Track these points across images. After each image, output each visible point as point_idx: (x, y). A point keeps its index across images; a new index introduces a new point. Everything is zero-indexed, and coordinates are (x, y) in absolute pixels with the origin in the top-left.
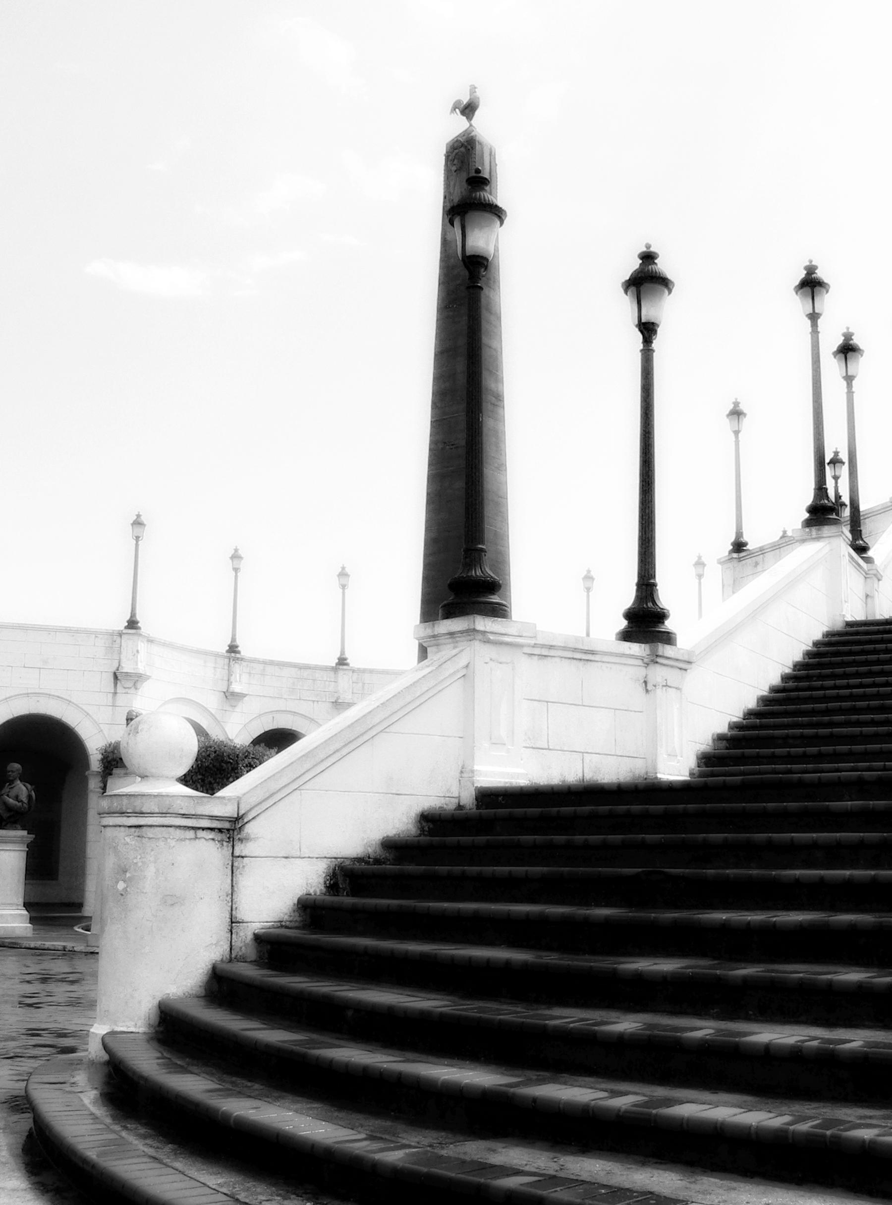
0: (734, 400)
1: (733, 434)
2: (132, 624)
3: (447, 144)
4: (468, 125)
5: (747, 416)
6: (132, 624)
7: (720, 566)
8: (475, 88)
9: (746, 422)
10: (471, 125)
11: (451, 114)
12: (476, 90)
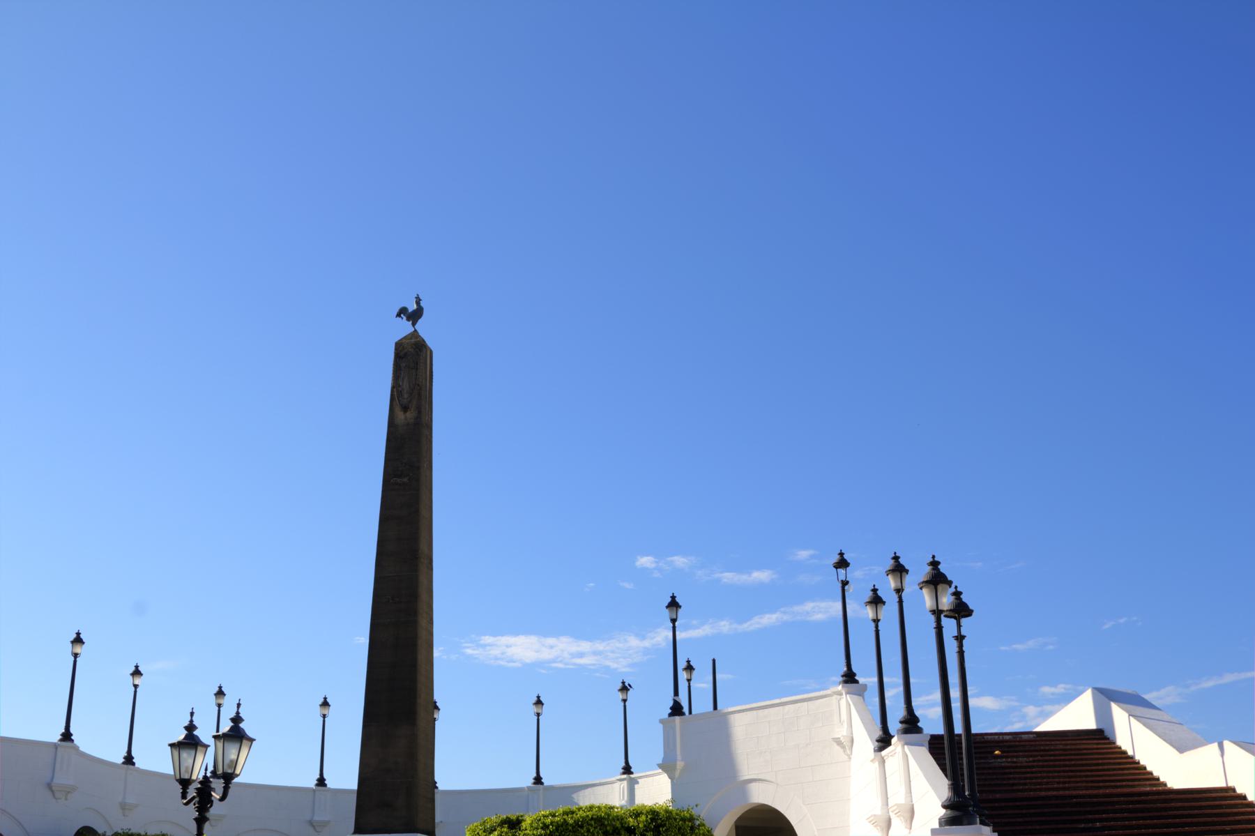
2: (67, 736)
3: (396, 344)
4: (413, 330)
6: (67, 736)
7: (661, 725)
9: (680, 611)
10: (415, 330)
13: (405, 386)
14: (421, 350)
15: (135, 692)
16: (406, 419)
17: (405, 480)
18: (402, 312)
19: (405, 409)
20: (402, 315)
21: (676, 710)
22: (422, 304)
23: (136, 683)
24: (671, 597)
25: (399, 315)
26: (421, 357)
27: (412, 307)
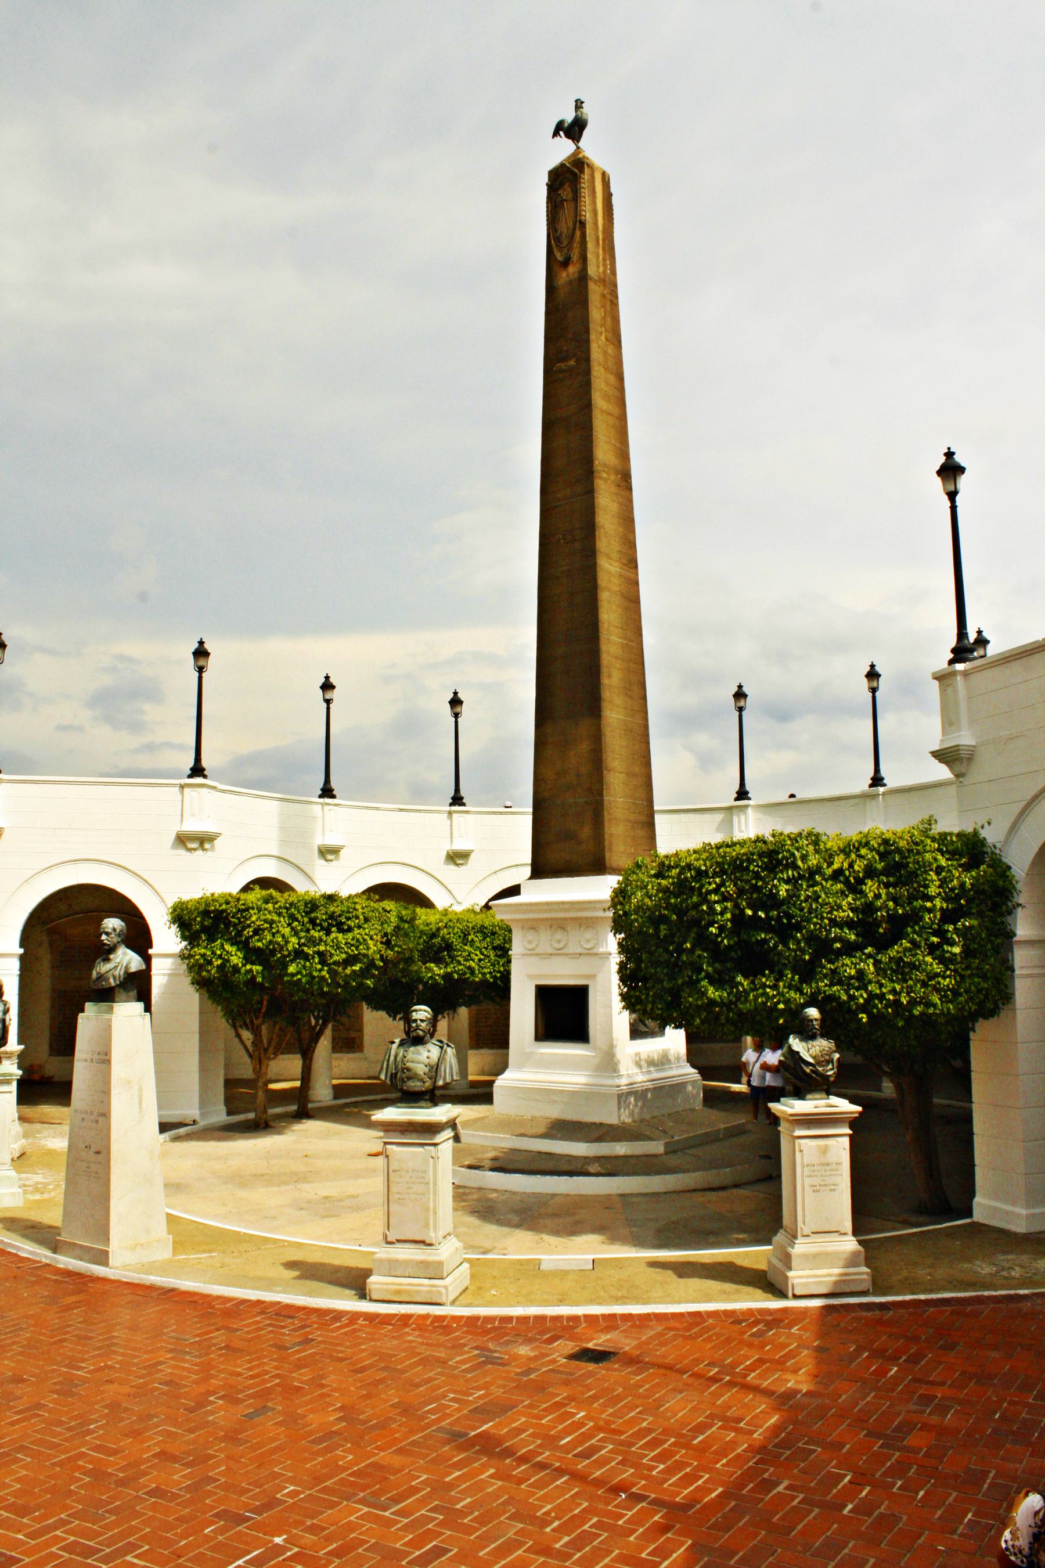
0: (947, 451)
1: (946, 497)
3: (550, 173)
4: (574, 147)
5: (966, 472)
7: (936, 683)
8: (582, 102)
10: (578, 148)
11: (553, 137)
12: (583, 105)
13: (565, 226)
14: (582, 171)
15: (328, 709)
16: (568, 275)
17: (572, 363)
18: (560, 128)
19: (566, 263)
20: (561, 133)
21: (961, 652)
22: (587, 110)
23: (327, 697)
24: (945, 454)
25: (556, 134)
26: (582, 181)
27: (569, 117)
